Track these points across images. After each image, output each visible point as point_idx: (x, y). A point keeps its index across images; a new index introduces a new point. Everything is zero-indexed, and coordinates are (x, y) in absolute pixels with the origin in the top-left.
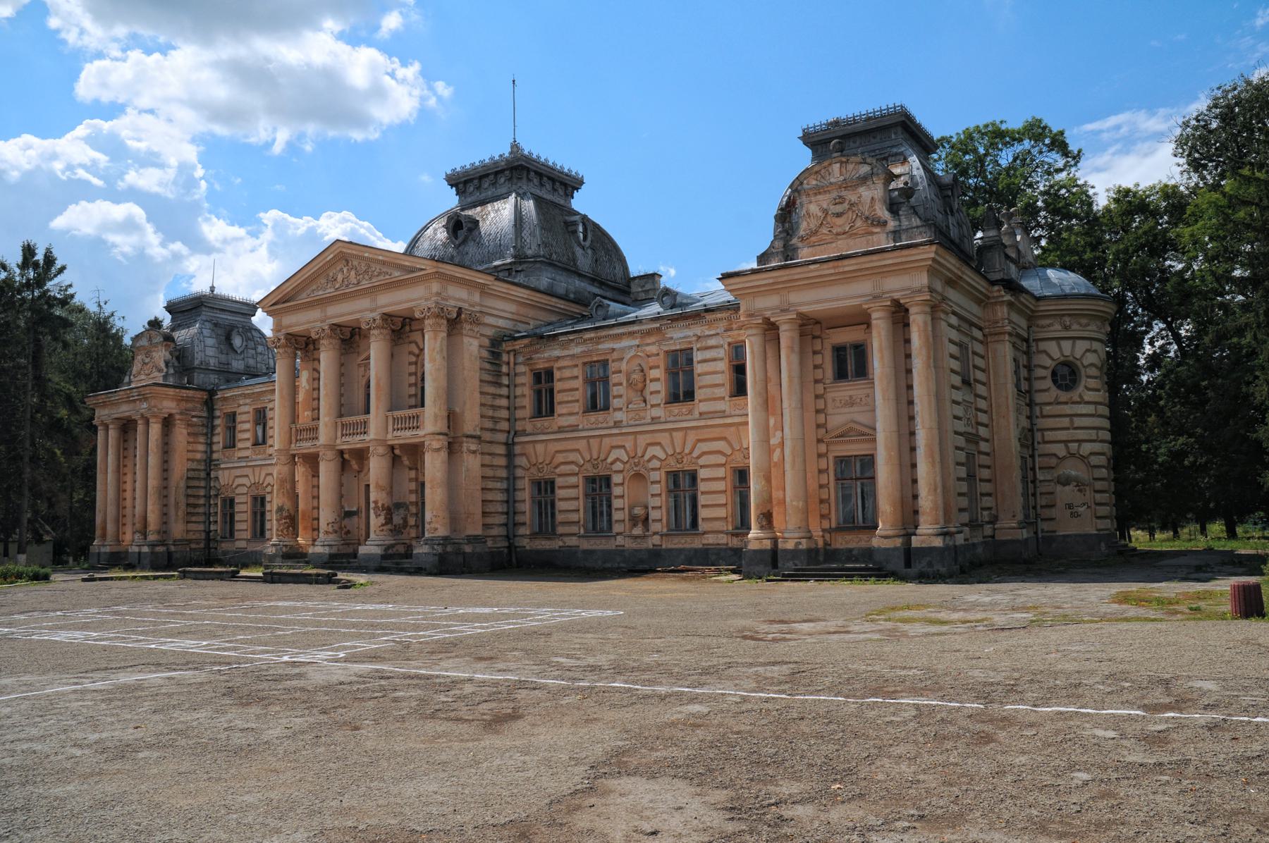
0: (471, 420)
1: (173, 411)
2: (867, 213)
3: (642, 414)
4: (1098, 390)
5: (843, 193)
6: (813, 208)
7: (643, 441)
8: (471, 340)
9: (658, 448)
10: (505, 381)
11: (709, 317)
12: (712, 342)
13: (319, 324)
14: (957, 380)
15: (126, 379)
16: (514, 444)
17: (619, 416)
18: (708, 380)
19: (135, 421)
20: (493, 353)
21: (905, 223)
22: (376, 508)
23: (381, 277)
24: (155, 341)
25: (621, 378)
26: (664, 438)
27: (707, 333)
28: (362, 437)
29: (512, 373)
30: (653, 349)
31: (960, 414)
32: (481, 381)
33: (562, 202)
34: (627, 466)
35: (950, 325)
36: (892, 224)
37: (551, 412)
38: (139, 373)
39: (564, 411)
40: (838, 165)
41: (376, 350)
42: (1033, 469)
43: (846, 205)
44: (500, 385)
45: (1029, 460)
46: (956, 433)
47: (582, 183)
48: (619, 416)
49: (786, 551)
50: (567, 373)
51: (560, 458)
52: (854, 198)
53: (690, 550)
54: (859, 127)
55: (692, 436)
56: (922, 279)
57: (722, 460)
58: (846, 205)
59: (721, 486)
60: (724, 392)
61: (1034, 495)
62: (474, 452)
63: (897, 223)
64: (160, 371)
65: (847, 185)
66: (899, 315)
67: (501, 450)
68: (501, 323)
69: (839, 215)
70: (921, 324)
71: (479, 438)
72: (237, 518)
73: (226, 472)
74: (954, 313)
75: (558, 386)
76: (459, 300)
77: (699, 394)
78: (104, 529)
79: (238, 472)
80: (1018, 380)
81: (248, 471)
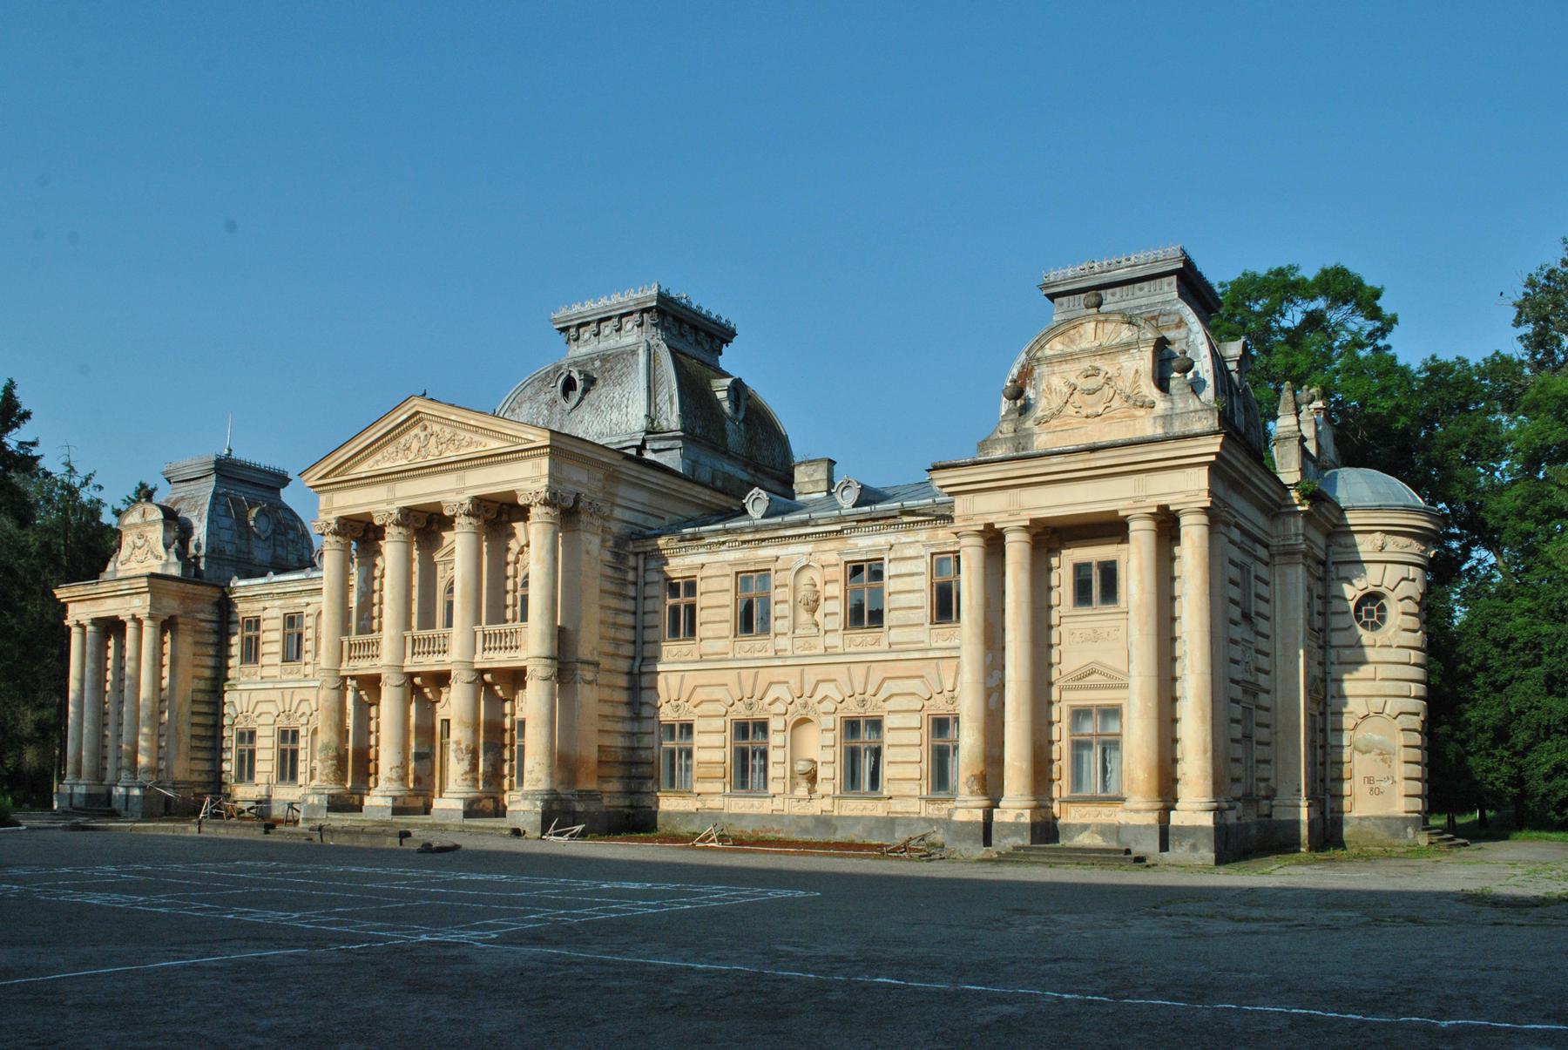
0: (589, 644)
1: (172, 612)
2: (1128, 391)
3: (813, 641)
4: (1415, 631)
5: (1098, 364)
6: (1057, 382)
7: (812, 675)
8: (591, 537)
9: (831, 685)
10: (631, 591)
13: (384, 507)
14: (1236, 613)
15: (110, 567)
16: (641, 673)
17: (783, 643)
18: (903, 600)
19: (123, 624)
20: (616, 555)
21: (1180, 406)
22: (459, 749)
24: (149, 518)
26: (839, 673)
27: (904, 540)
28: (441, 657)
29: (641, 582)
30: (832, 558)
31: (1238, 657)
32: (602, 591)
33: (707, 359)
34: (791, 708)
35: (1232, 542)
36: (1162, 405)
37: (692, 631)
38: (128, 560)
39: (709, 634)
40: (1093, 325)
41: (459, 543)
42: (1323, 730)
43: (1100, 379)
44: (625, 597)
45: (1319, 719)
46: (1233, 681)
47: (733, 334)
48: (783, 643)
50: (714, 584)
51: (701, 694)
52: (1112, 371)
53: (870, 818)
55: (877, 673)
56: (1199, 480)
58: (1100, 379)
59: (915, 737)
60: (925, 613)
61: (1323, 764)
62: (590, 683)
63: (1169, 405)
64: (158, 557)
65: (1102, 352)
66: (1167, 524)
67: (623, 681)
68: (628, 515)
69: (1091, 392)
70: (1196, 538)
71: (597, 664)
72: (258, 756)
73: (245, 695)
74: (1238, 526)
75: (700, 601)
76: (578, 483)
77: (888, 618)
78: (79, 762)
79: (261, 696)
80: (1311, 615)
81: (276, 695)
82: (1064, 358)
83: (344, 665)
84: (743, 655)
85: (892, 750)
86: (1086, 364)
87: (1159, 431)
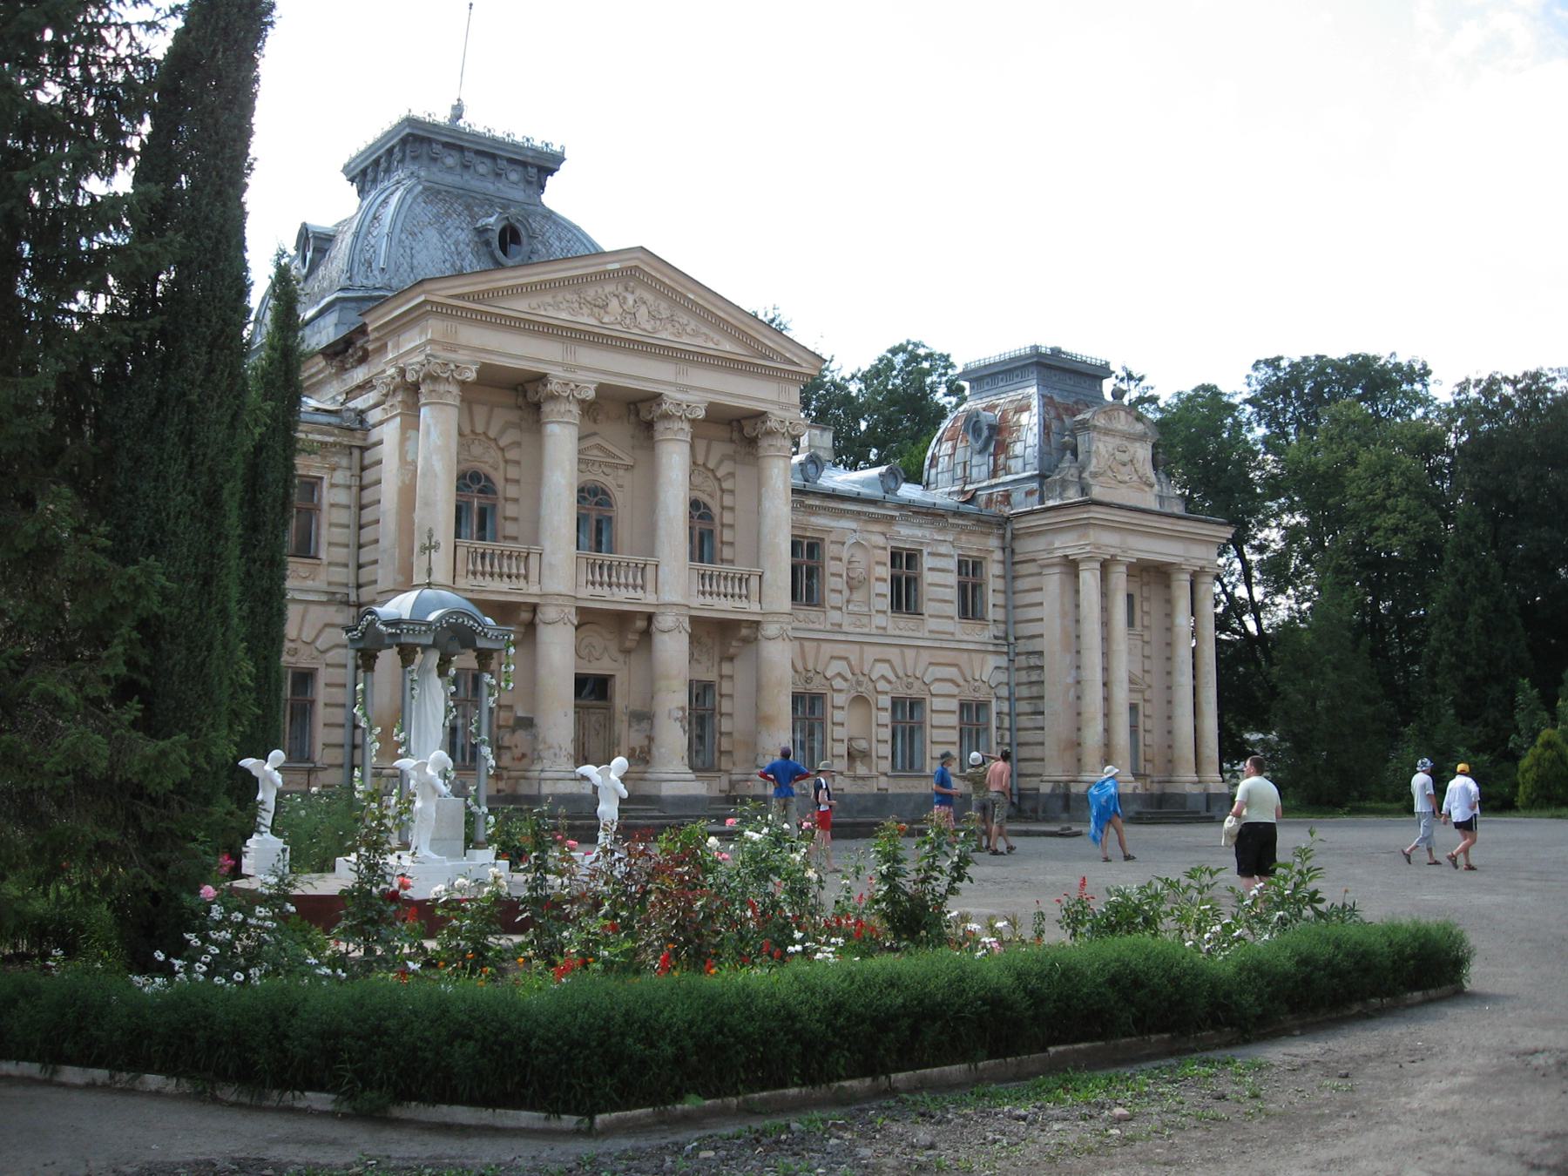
12: (943, 549)
26: (893, 654)
30: (881, 541)
49: (1077, 795)
54: (1075, 366)
57: (955, 691)
82: (1107, 432)
84: (898, 632)
85: (935, 731)
86: (1118, 441)
87: (1155, 506)
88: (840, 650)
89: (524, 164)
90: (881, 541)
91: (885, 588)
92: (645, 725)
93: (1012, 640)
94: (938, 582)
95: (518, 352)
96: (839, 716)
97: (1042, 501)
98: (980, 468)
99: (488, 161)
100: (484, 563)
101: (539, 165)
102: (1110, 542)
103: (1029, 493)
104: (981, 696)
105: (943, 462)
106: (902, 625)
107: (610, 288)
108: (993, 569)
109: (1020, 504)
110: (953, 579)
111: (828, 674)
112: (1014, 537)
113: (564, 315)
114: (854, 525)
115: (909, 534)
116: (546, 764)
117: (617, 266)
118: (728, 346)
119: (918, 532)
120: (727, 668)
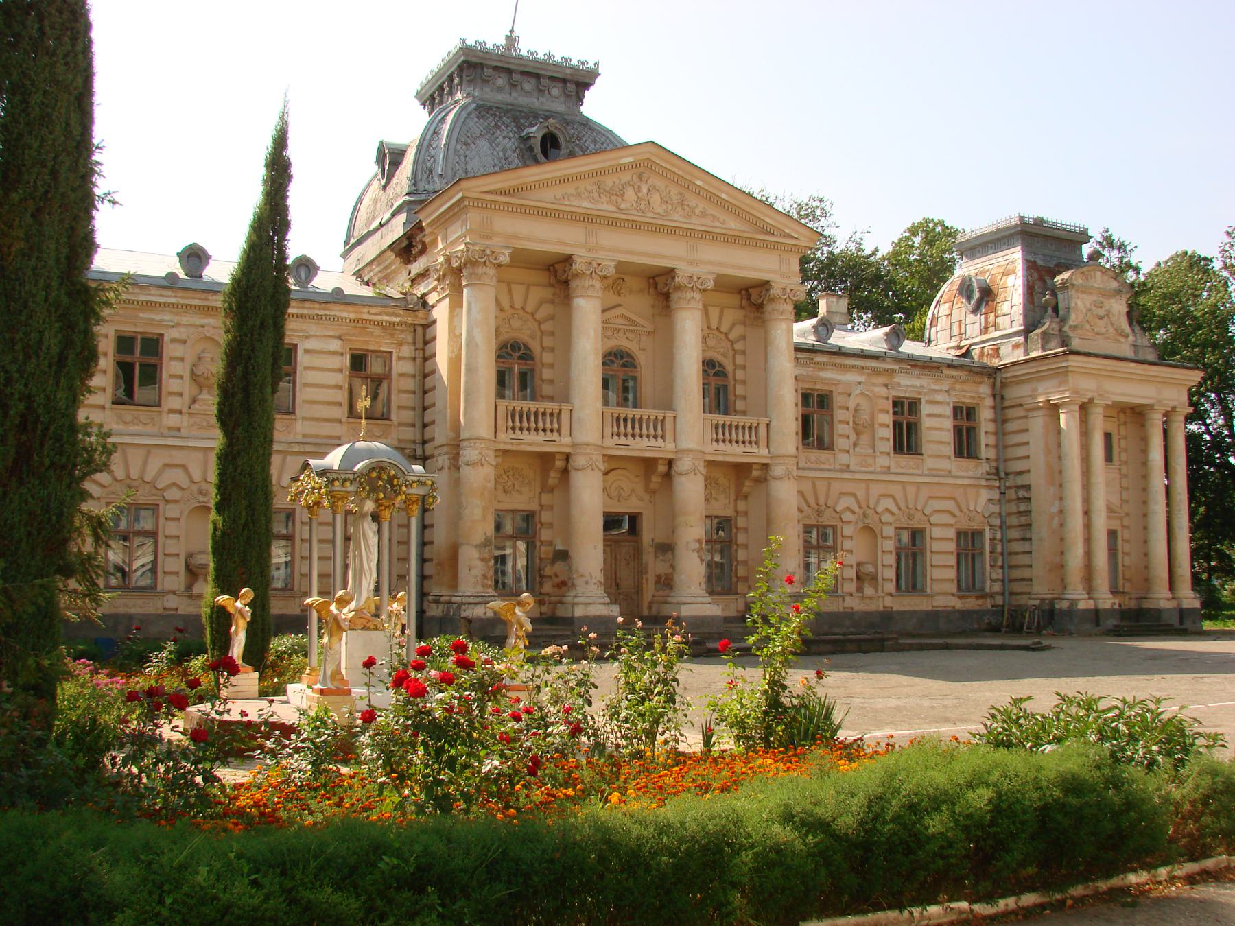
11: (947, 372)
12: (939, 398)
23: (707, 221)
25: (847, 416)
27: (933, 387)
48: (843, 458)
49: (1061, 610)
55: (925, 492)
57: (952, 521)
69: (1101, 318)
82: (1085, 290)
83: (502, 436)
84: (899, 470)
86: (1094, 298)
87: (1129, 354)
88: (848, 487)
89: (564, 81)
90: (883, 391)
91: (888, 433)
92: (669, 555)
93: (1003, 475)
94: (937, 427)
95: (548, 237)
96: (847, 544)
97: (1027, 352)
98: (974, 324)
99: (533, 81)
100: (518, 420)
101: (577, 81)
102: (1087, 386)
103: (1016, 346)
104: (975, 526)
105: (943, 322)
106: (903, 464)
107: (626, 177)
108: (985, 415)
109: (1008, 355)
110: (948, 424)
111: (838, 509)
112: (1003, 385)
113: (585, 204)
114: (862, 379)
115: (908, 384)
116: (580, 590)
117: (630, 159)
118: (733, 224)
119: (917, 382)
120: (741, 506)
